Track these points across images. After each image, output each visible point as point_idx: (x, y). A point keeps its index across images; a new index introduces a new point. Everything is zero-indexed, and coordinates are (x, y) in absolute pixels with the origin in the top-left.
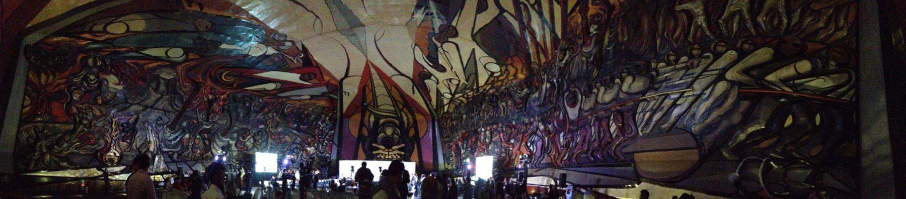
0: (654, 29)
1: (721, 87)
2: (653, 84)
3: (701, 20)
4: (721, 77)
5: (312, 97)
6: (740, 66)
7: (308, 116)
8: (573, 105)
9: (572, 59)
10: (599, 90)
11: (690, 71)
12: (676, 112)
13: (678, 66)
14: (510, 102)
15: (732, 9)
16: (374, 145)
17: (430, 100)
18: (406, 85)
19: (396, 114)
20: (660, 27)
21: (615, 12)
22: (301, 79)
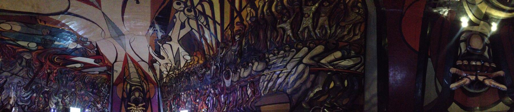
0: (265, 37)
1: (301, 67)
2: (267, 67)
3: (289, 32)
4: (300, 62)
5: (100, 73)
6: (309, 55)
7: (98, 84)
8: (228, 78)
9: (227, 52)
10: (241, 70)
11: (285, 59)
12: (280, 81)
13: (279, 56)
14: (195, 77)
15: (304, 26)
16: (129, 103)
17: (156, 75)
18: (145, 67)
19: (141, 83)
20: (269, 36)
21: (247, 29)
22: (95, 62)
